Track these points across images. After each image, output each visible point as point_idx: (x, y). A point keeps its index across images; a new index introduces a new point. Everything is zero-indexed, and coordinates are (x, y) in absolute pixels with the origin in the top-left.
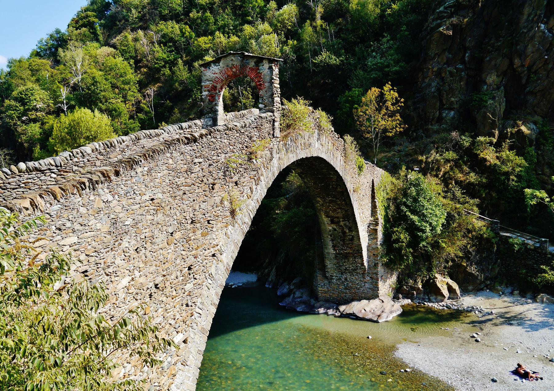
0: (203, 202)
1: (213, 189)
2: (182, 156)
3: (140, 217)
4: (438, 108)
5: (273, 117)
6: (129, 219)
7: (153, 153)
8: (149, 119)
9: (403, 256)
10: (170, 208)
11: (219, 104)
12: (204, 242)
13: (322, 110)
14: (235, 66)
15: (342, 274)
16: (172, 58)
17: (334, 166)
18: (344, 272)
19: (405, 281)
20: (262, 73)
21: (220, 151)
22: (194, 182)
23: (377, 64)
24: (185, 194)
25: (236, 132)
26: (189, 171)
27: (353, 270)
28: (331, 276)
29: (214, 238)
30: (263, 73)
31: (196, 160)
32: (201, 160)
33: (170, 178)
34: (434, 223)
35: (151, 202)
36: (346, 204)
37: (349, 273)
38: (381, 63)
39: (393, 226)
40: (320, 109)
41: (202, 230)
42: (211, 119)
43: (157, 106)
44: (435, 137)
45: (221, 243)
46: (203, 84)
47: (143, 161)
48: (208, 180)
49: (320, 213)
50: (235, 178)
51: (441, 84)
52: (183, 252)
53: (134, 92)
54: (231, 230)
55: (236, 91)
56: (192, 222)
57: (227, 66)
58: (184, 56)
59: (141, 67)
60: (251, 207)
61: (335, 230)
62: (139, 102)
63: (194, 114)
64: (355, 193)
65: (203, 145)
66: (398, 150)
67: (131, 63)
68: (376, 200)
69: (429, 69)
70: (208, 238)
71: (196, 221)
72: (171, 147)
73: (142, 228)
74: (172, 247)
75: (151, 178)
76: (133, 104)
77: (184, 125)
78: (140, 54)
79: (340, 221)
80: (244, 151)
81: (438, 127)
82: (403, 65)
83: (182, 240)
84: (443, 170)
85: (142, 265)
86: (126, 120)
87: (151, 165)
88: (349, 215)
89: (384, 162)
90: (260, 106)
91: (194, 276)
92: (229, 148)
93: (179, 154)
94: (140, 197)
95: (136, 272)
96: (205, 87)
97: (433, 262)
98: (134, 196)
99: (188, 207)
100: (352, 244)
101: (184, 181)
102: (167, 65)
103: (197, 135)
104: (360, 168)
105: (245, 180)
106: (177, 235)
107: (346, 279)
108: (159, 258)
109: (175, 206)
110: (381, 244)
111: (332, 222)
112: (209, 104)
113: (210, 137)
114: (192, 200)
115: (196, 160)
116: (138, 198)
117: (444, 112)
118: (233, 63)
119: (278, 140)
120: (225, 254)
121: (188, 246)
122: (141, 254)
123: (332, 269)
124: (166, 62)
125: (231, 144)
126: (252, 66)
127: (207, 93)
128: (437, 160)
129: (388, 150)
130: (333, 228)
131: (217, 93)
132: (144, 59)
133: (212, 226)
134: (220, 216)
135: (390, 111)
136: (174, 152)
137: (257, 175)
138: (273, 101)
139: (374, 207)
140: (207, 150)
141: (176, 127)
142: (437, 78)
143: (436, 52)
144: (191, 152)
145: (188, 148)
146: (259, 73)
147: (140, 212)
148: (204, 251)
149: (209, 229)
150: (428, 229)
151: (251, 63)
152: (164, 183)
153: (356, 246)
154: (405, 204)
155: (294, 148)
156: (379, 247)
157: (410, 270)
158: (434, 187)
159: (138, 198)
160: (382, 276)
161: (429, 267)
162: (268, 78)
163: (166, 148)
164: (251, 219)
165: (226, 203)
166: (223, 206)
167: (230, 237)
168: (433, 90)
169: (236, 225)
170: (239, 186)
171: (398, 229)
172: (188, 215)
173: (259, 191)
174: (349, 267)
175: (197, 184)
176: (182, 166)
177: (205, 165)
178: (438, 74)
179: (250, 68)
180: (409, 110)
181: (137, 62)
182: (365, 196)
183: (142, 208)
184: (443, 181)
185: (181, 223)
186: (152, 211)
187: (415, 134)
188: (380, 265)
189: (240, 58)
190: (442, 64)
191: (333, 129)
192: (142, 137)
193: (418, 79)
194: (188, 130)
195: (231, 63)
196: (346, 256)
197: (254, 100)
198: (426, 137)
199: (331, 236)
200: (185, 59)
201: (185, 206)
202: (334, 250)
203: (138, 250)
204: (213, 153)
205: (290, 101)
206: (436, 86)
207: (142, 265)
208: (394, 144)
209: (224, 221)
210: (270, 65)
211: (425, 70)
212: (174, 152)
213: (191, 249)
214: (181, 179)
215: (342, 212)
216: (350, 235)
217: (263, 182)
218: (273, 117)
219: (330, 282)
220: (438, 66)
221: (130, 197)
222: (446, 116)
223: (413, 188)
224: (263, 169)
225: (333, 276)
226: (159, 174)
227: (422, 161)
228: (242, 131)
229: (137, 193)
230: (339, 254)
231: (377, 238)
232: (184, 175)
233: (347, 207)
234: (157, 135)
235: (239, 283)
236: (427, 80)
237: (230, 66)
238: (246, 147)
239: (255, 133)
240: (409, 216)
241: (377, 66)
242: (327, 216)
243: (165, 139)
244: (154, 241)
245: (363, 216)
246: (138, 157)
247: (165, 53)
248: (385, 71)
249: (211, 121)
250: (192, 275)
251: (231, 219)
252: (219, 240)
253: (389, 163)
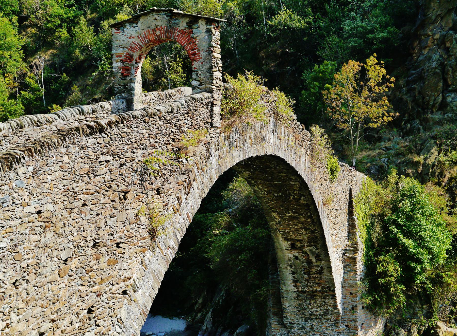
0: (111, 217)
1: (125, 199)
2: (82, 151)
3: (20, 236)
4: (442, 90)
5: (212, 99)
6: (5, 239)
7: (41, 146)
8: (36, 100)
9: (392, 295)
10: (64, 224)
11: (137, 79)
12: (111, 273)
13: (281, 90)
14: (159, 27)
15: (306, 320)
16: (71, 14)
17: (296, 169)
18: (309, 318)
19: (395, 331)
20: (196, 38)
21: (135, 145)
22: (98, 188)
23: (357, 28)
24: (85, 205)
25: (159, 119)
26: (92, 173)
27: (322, 315)
28: (291, 323)
29: (126, 267)
30: (198, 38)
31: (102, 158)
32: (109, 158)
33: (65, 182)
34: (436, 249)
35: (37, 216)
36: (313, 222)
37: (316, 319)
38: (362, 27)
39: (377, 254)
40: (277, 88)
41: (108, 257)
42: (124, 100)
43: (47, 82)
44: (437, 130)
45: (135, 275)
46: (113, 51)
47: (27, 158)
48: (118, 186)
49: (276, 235)
50: (157, 184)
51: (446, 57)
52: (81, 288)
53: (17, 61)
54: (150, 257)
55: (160, 62)
56: (95, 246)
57: (149, 27)
58: (89, 12)
59: (27, 27)
60: (178, 225)
61: (297, 258)
62: (24, 75)
63: (101, 92)
64: (326, 207)
65: (112, 137)
66: (386, 147)
67: (14, 21)
68: (354, 217)
69: (429, 36)
70: (117, 268)
71: (100, 244)
72: (67, 139)
73: (23, 253)
74: (66, 280)
75: (37, 182)
76: (15, 78)
77: (87, 108)
78: (26, 8)
79: (304, 246)
80: (169, 147)
81: (441, 116)
82: (392, 29)
83: (79, 270)
84: (448, 175)
85: (21, 305)
86: (4, 100)
87: (38, 164)
88: (316, 237)
89: (367, 163)
90: (194, 83)
91: (96, 321)
92: (148, 142)
93: (77, 149)
94: (21, 209)
95: (13, 316)
96: (117, 56)
97: (434, 304)
98: (13, 208)
99: (90, 224)
100: (321, 278)
101: (84, 187)
102: (65, 24)
103: (103, 122)
104: (333, 172)
105: (171, 186)
106: (74, 263)
107: (312, 328)
108: (47, 295)
109: (71, 222)
110: (361, 278)
111: (293, 247)
112: (122, 79)
113: (122, 125)
114: (95, 214)
115: (102, 158)
116: (18, 210)
117: (448, 96)
119: (218, 131)
120: (140, 291)
121: (88, 278)
122: (20, 290)
123: (293, 313)
124: (63, 21)
125: (151, 136)
126: (183, 28)
127: (119, 64)
128: (440, 163)
129: (371, 146)
130: (294, 256)
131: (133, 65)
132: (32, 16)
133: (123, 251)
134: (134, 238)
135: (374, 93)
136: (70, 145)
137: (187, 180)
138: (212, 76)
139: (352, 226)
140: (117, 144)
141: (74, 111)
142: (439, 48)
143: (439, 13)
144: (95, 146)
145: (92, 140)
146: (193, 38)
147: (21, 229)
148: (110, 286)
149: (119, 255)
150: (426, 258)
151: (181, 24)
152: (56, 190)
153: (326, 282)
154: (395, 222)
155: (239, 143)
156: (359, 282)
157: (402, 316)
158: (435, 199)
159: (18, 210)
160: (362, 324)
161: (428, 312)
162: (204, 46)
163: (60, 141)
164: (178, 241)
165: (144, 219)
166: (139, 222)
167: (148, 266)
168: (434, 65)
169: (157, 250)
170: (162, 195)
171: (386, 258)
172: (89, 235)
173: (190, 203)
174: (316, 311)
175: (102, 192)
176: (82, 165)
177: (115, 165)
178: (442, 43)
179: (179, 31)
180: (400, 93)
181: (22, 19)
182: (340, 211)
183: (23, 225)
184: (448, 191)
185: (78, 246)
186: (39, 228)
187: (409, 125)
188: (360, 307)
189: (167, 16)
190: (447, 29)
191: (295, 117)
192: (27, 125)
193: (414, 49)
194: (91, 116)
195: (154, 23)
196: (312, 296)
197: (185, 75)
198: (425, 129)
199: (291, 266)
200: (89, 16)
201: (85, 222)
202: (296, 286)
203: (17, 284)
204: (125, 148)
205: (235, 77)
206: (439, 60)
207: (21, 305)
208: (380, 139)
209: (140, 244)
210: (208, 27)
211: (423, 38)
212: (70, 145)
213: (92, 283)
214: (80, 184)
215: (306, 234)
216: (317, 266)
217: (196, 190)
218: (212, 99)
219: (289, 332)
220: (440, 32)
221: (7, 209)
222: (451, 102)
223: (407, 201)
224: (196, 171)
225: (293, 324)
226: (49, 177)
227: (418, 163)
228: (168, 118)
229: (17, 202)
230: (302, 292)
231: (355, 271)
232: (85, 178)
233: (314, 226)
234: (48, 122)
235: (160, 332)
236: (425, 52)
237: (153, 27)
238: (173, 140)
239: (186, 121)
240: (401, 240)
241: (357, 31)
242: (287, 239)
243: (59, 128)
244: (39, 271)
245: (337, 239)
246: (19, 152)
247: (61, 8)
248: (368, 38)
249: (125, 104)
250: (93, 321)
251: (150, 241)
252: (133, 271)
253: (373, 165)
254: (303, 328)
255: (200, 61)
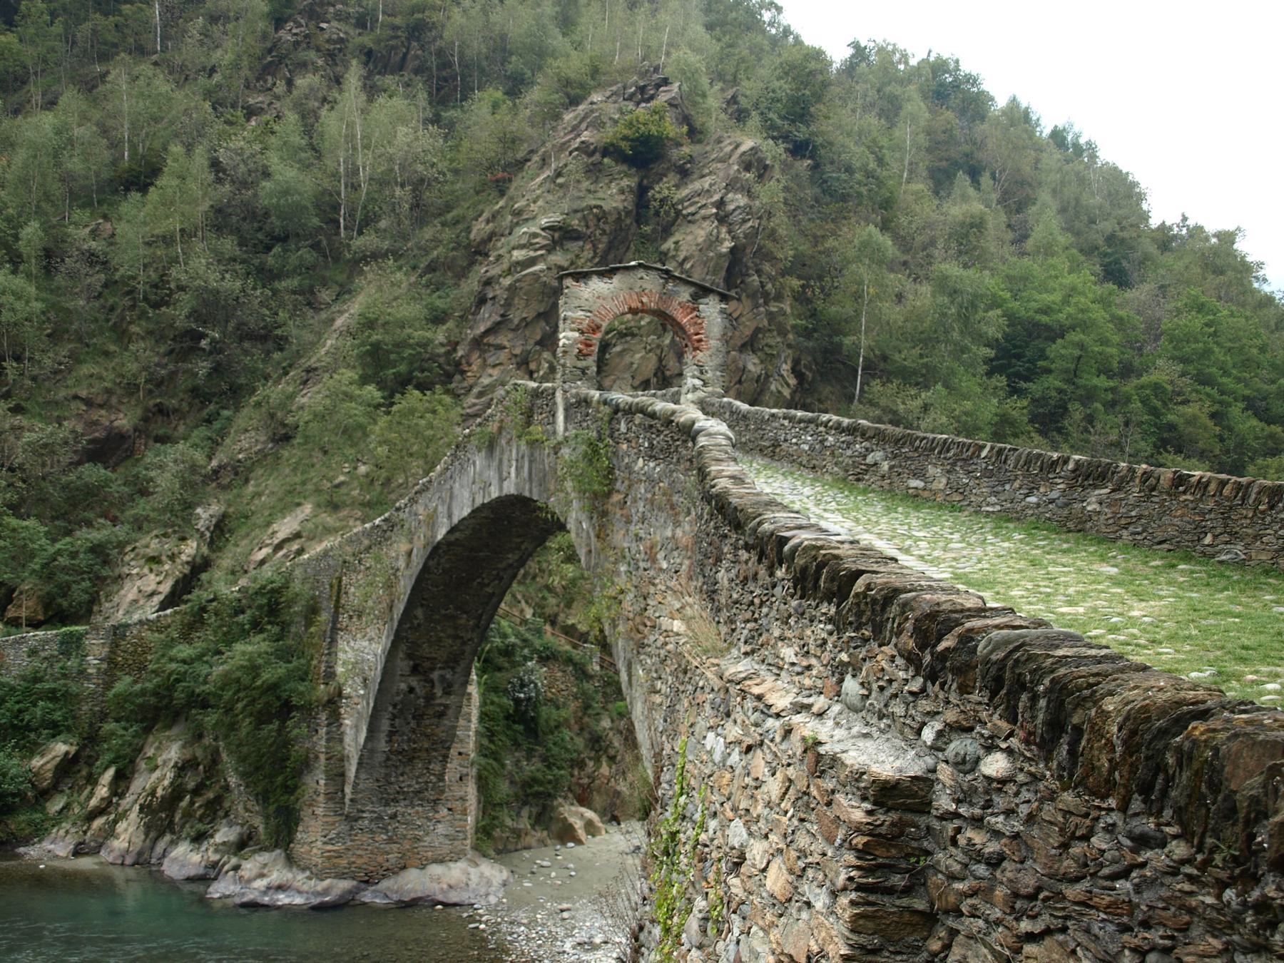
15: (387, 805)
61: (411, 690)
118: (645, 286)
143: (524, 315)
190: (532, 342)
193: (470, 365)
199: (395, 706)
202: (389, 741)
219: (352, 828)
242: (410, 656)
254: (380, 818)
255: (708, 353)
